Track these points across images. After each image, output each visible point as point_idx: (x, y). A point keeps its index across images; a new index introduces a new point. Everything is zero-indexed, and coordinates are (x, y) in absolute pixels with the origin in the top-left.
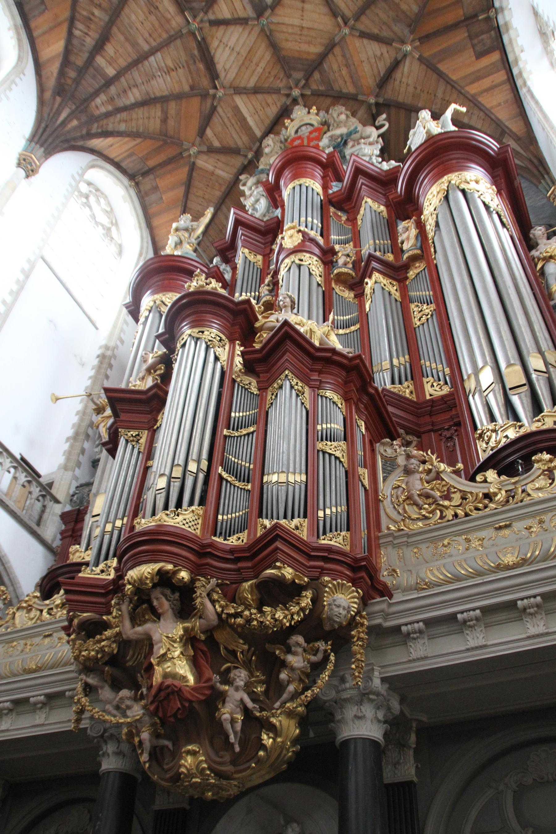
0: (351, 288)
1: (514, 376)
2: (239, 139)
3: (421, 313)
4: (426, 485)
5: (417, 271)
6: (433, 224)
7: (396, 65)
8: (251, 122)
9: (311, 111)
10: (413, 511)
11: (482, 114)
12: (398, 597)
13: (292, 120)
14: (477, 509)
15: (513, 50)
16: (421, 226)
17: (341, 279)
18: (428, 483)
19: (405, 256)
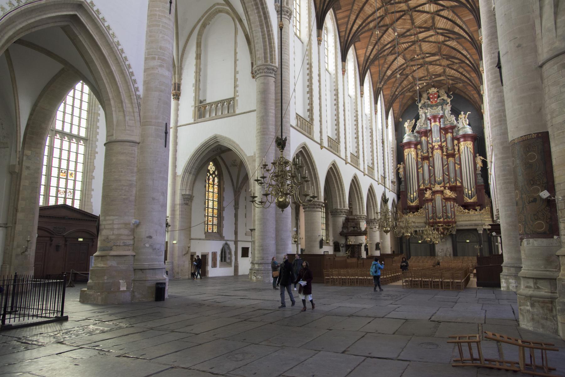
1: (470, 192)
3: (457, 167)
16: (459, 147)
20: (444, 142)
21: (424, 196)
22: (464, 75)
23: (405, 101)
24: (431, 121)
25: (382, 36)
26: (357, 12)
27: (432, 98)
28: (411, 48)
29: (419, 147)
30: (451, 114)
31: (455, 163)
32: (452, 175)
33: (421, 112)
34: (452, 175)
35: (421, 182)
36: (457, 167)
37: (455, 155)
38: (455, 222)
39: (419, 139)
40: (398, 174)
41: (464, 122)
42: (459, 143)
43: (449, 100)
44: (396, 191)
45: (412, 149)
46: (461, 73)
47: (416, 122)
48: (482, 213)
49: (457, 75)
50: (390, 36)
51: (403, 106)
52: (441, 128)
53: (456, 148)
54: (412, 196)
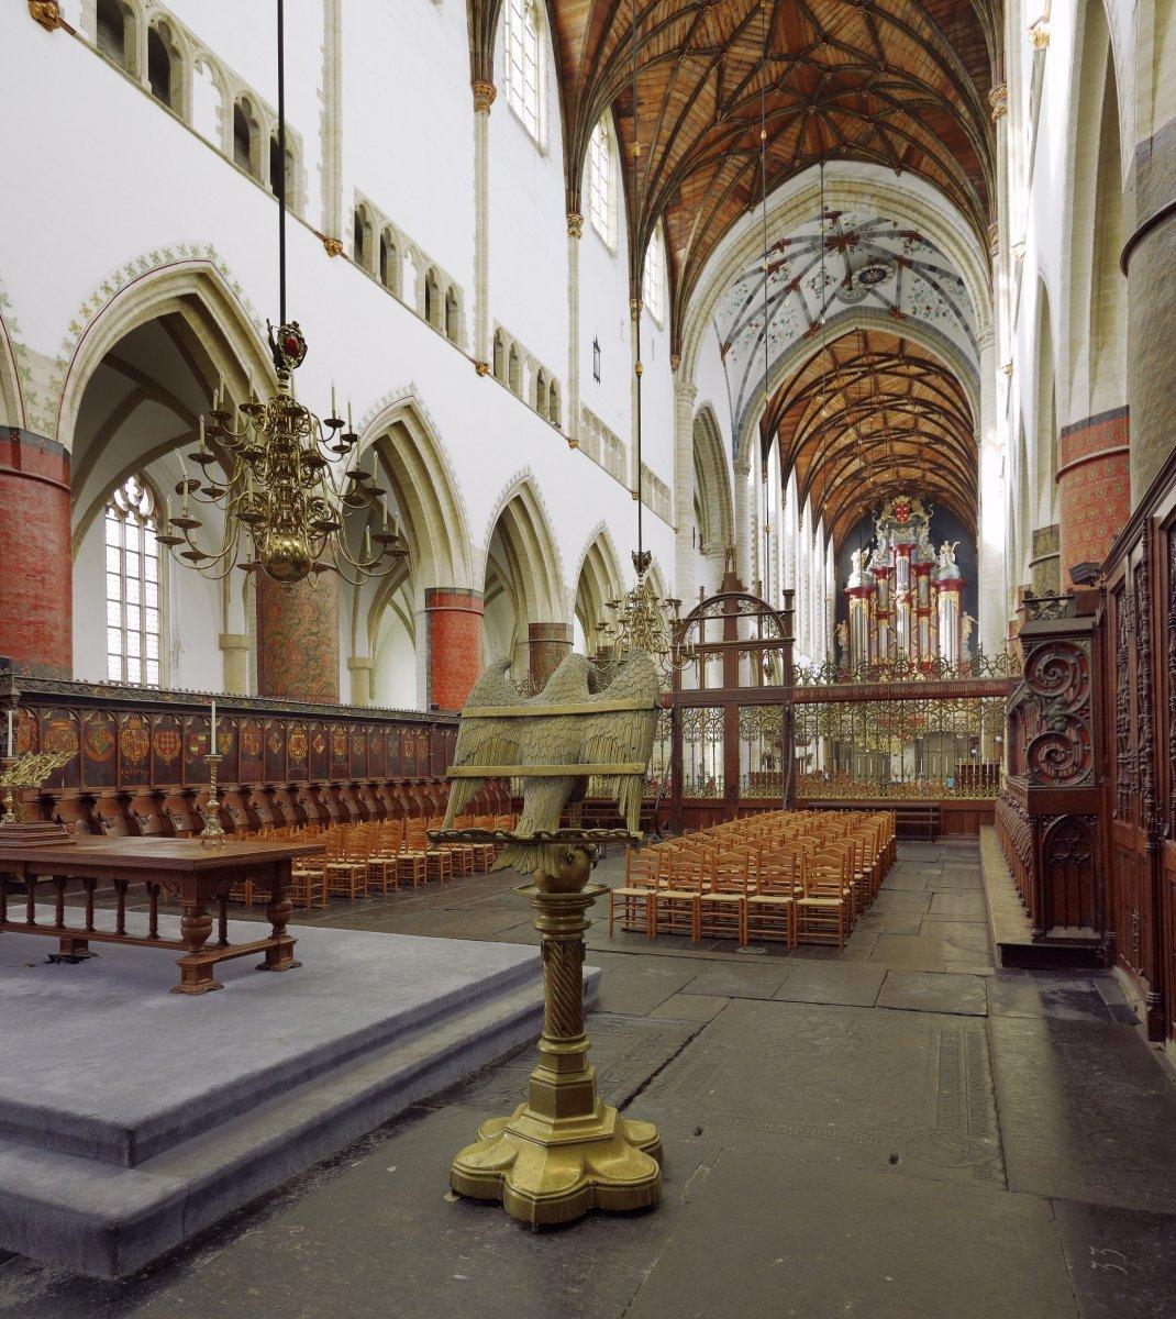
3: (933, 631)
22: (954, 486)
25: (837, 438)
26: (809, 417)
28: (877, 448)
30: (929, 542)
31: (930, 625)
33: (880, 535)
37: (930, 612)
40: (836, 639)
42: (938, 592)
43: (926, 519)
46: (950, 483)
47: (871, 552)
49: (943, 483)
50: (851, 436)
51: (849, 528)
52: (910, 566)
53: (933, 601)
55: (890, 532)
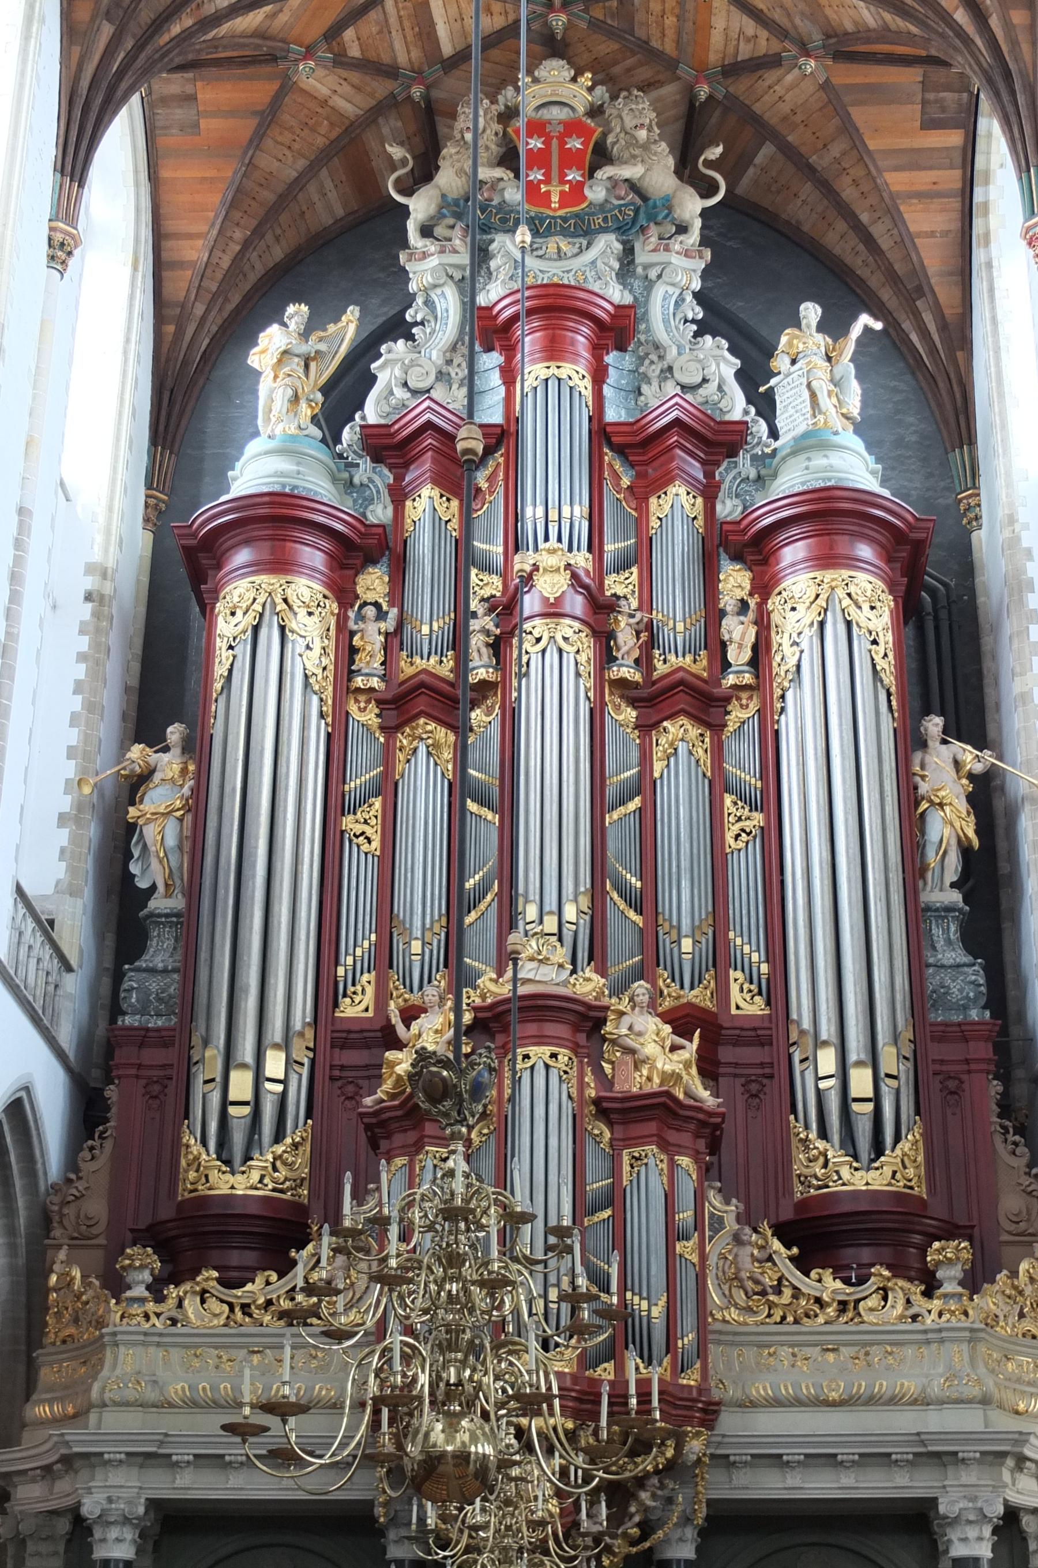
0: (633, 702)
1: (861, 1082)
2: (402, 51)
3: (741, 822)
4: (756, 1264)
5: (744, 715)
6: (792, 661)
7: (774, 61)
8: (442, 31)
9: (581, 80)
10: (740, 1297)
11: (895, 232)
12: (729, 1422)
13: (536, 81)
14: (808, 1316)
15: (989, 153)
16: (764, 624)
17: (622, 684)
18: (760, 1261)
19: (731, 680)
20: (622, 565)
21: (374, 1073)
23: (282, 163)
24: (510, 350)
27: (539, 159)
29: (373, 583)
30: (703, 328)
31: (718, 784)
32: (684, 899)
34: (684, 899)
35: (358, 944)
36: (741, 822)
38: (708, 1412)
39: (380, 513)
41: (823, 387)
43: (692, 206)
44: (67, 1035)
45: (305, 588)
47: (366, 350)
48: (991, 1321)
52: (601, 433)
53: (739, 633)
54: (241, 1085)
55: (481, 255)
